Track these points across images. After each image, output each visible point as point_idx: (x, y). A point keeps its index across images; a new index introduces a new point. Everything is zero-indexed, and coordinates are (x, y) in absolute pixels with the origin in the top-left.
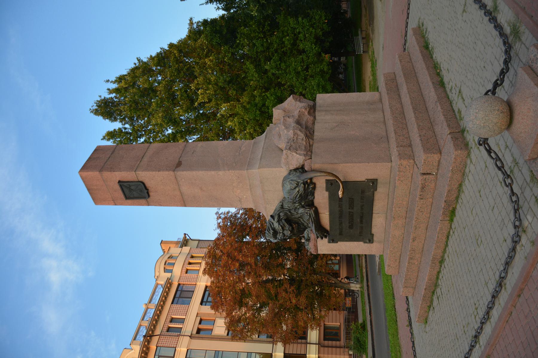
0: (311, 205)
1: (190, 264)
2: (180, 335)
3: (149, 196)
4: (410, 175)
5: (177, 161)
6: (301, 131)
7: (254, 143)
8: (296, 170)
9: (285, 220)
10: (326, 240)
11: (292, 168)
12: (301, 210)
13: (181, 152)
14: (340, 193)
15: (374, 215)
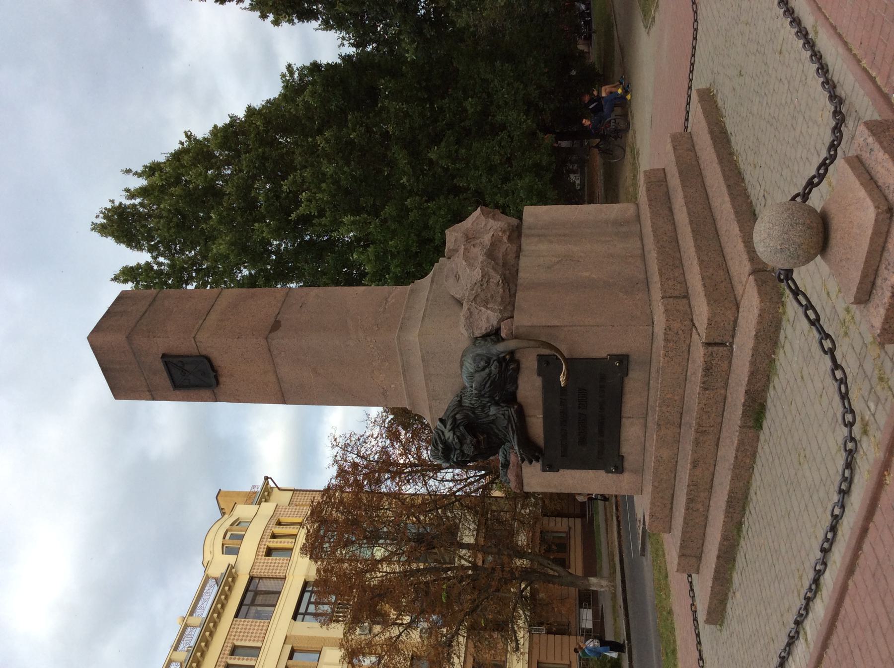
0: (511, 399)
1: (274, 536)
3: (218, 383)
4: (685, 348)
5: (273, 320)
6: (494, 269)
7: (412, 291)
8: (485, 337)
9: (466, 427)
10: (537, 466)
11: (478, 333)
12: (493, 410)
13: (279, 305)
14: (562, 378)
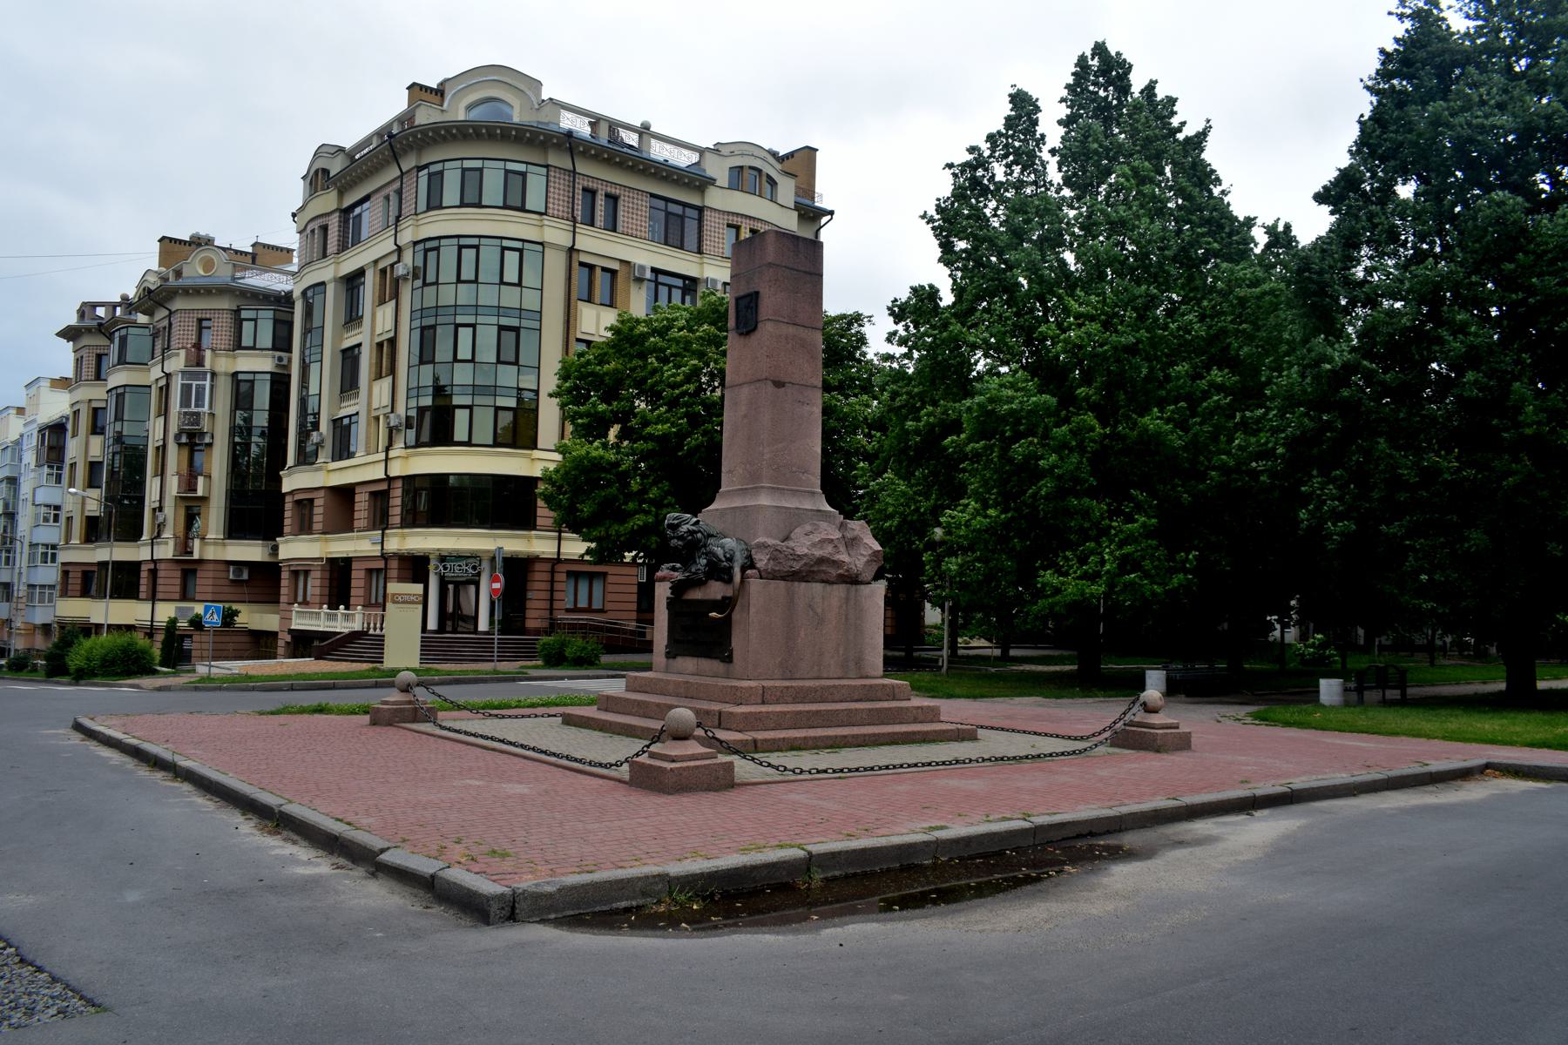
2: (574, 221)
7: (813, 493)
8: (750, 557)
14: (713, 614)
15: (695, 660)
